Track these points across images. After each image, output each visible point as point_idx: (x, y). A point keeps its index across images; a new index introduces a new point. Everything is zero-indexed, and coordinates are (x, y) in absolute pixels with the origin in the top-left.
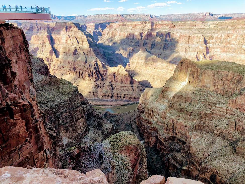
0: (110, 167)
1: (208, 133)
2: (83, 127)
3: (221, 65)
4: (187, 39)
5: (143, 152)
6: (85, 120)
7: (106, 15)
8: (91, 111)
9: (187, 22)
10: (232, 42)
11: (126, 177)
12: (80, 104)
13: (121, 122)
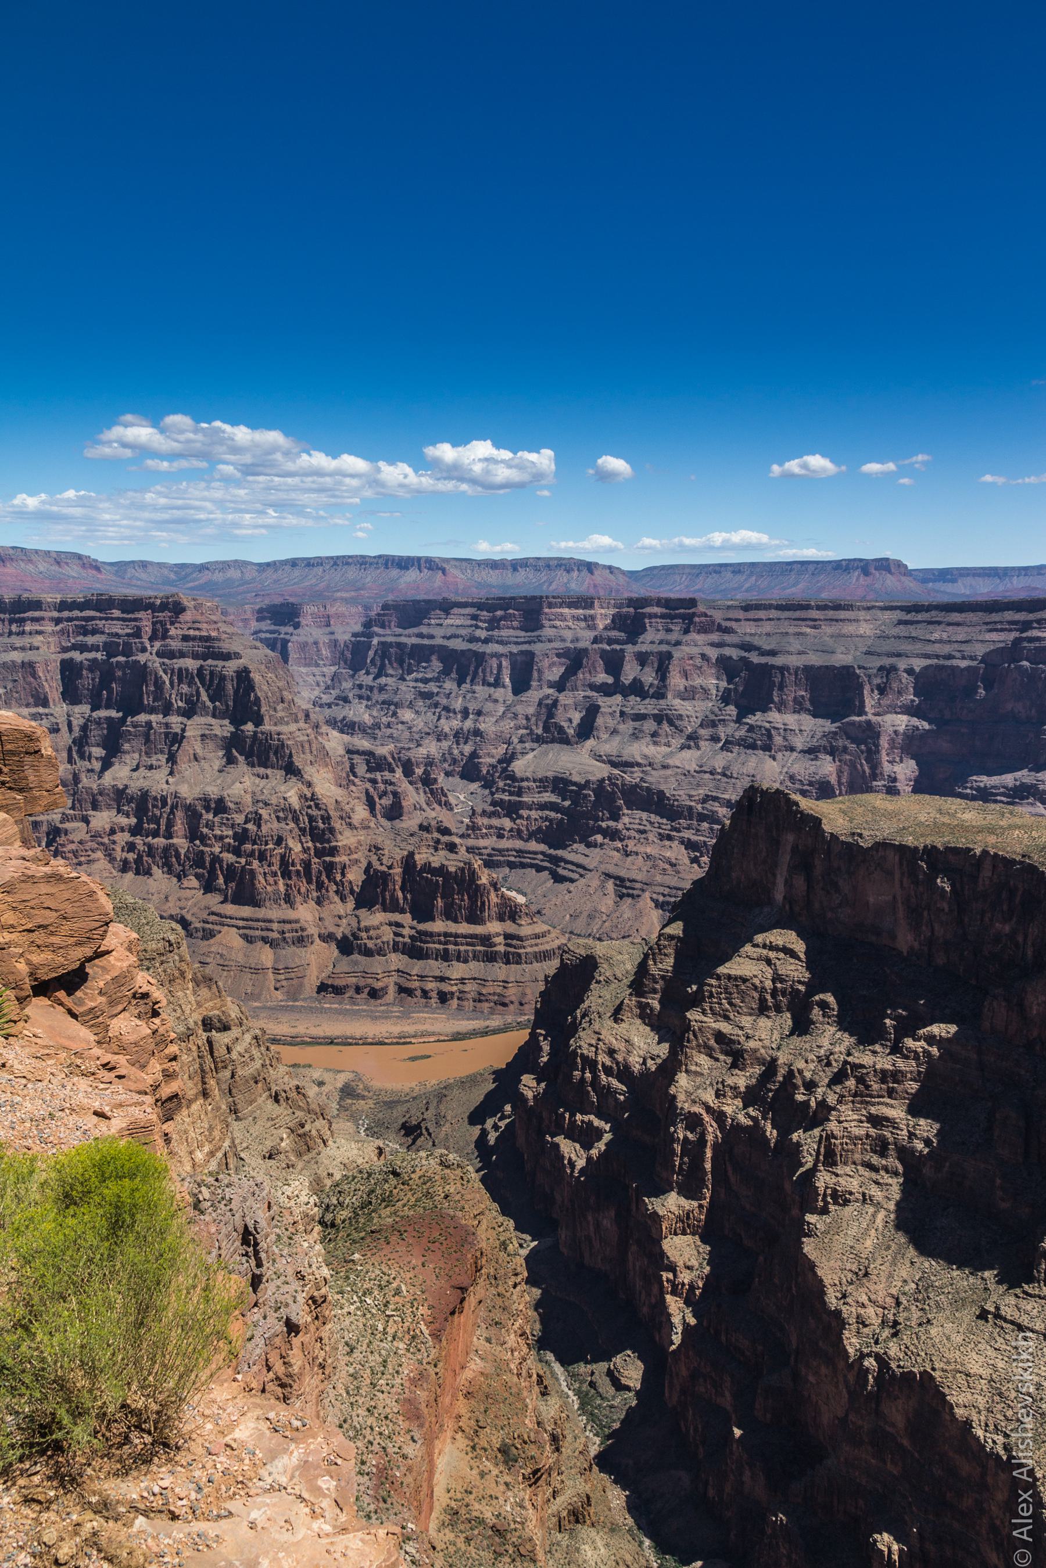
0: (299, 1298)
1: (890, 1181)
2: (206, 1149)
3: (946, 820)
5: (508, 1259)
6: (219, 1108)
8: (258, 1064)
11: (397, 1372)
12: (191, 1020)
13: (430, 1134)
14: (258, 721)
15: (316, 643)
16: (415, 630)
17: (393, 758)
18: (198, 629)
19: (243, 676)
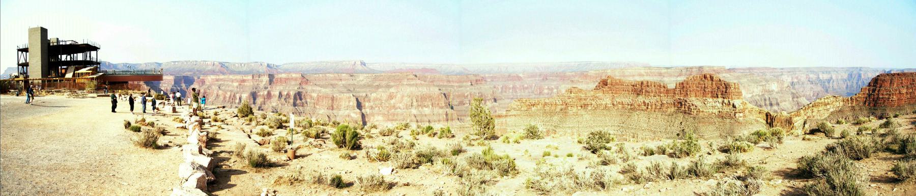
4: (330, 101)
7: (195, 63)
9: (328, 75)
10: (398, 105)
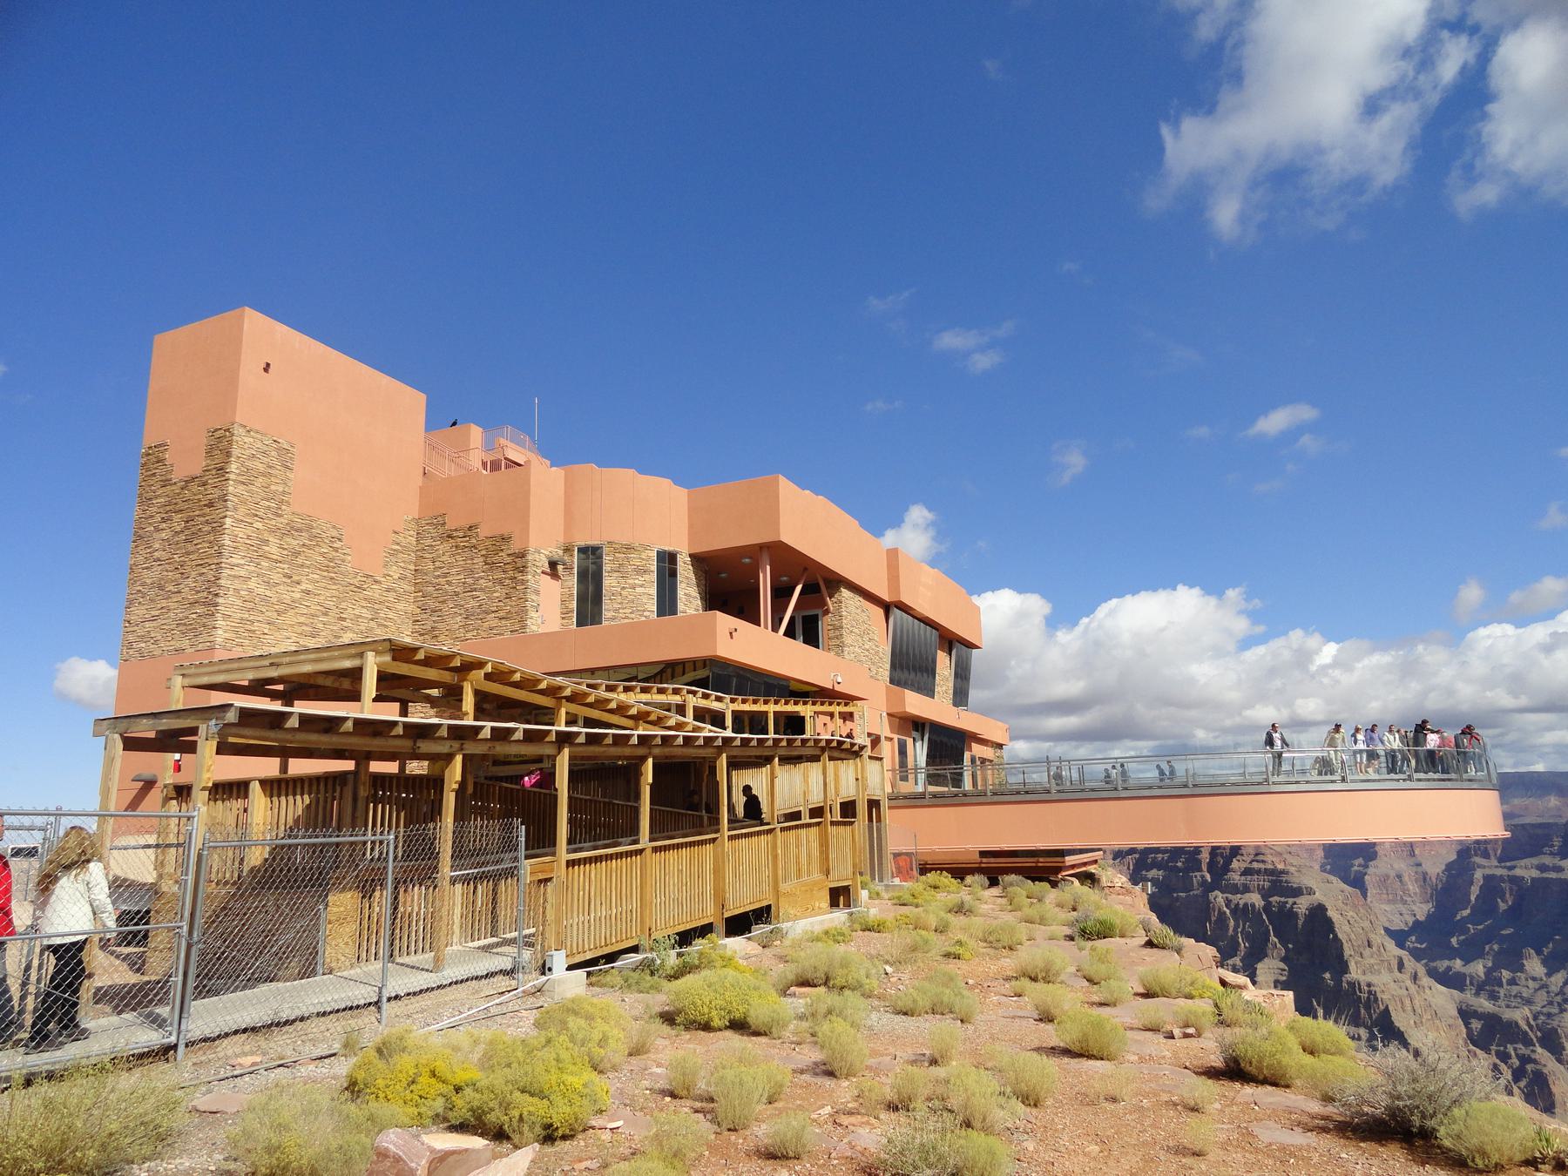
14: (1343, 967)
15: (1399, 877)
16: (1535, 861)
17: (1531, 1027)
18: (1263, 861)
19: (1318, 912)
